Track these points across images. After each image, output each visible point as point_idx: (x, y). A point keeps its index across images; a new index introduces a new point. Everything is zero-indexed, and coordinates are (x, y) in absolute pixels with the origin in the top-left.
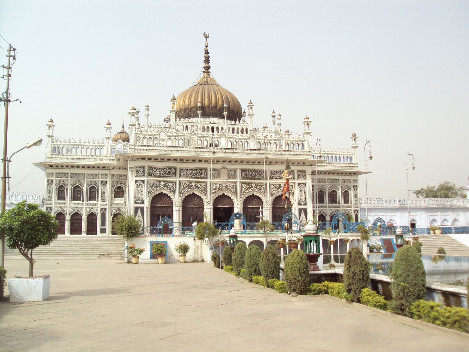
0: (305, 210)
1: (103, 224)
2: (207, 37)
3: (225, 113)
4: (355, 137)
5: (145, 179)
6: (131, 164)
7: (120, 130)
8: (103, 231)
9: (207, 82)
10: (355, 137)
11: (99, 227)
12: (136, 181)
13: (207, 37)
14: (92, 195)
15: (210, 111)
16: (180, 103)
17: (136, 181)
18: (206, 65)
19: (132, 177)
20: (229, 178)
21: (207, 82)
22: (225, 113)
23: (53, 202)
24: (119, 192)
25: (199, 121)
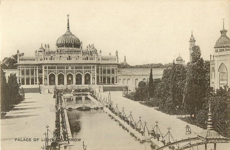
0: (94, 77)
1: (36, 81)
2: (68, 16)
3: (73, 46)
4: (117, 52)
5: (47, 70)
6: (43, 66)
7: (41, 47)
8: (36, 84)
9: (69, 33)
10: (117, 52)
11: (35, 82)
12: (45, 70)
13: (68, 16)
14: (32, 74)
15: (68, 45)
16: (60, 42)
17: (45, 70)
18: (68, 26)
19: (43, 70)
20: (71, 69)
21: (69, 33)
22: (73, 46)
23: (21, 75)
24: (41, 72)
25: (64, 48)
